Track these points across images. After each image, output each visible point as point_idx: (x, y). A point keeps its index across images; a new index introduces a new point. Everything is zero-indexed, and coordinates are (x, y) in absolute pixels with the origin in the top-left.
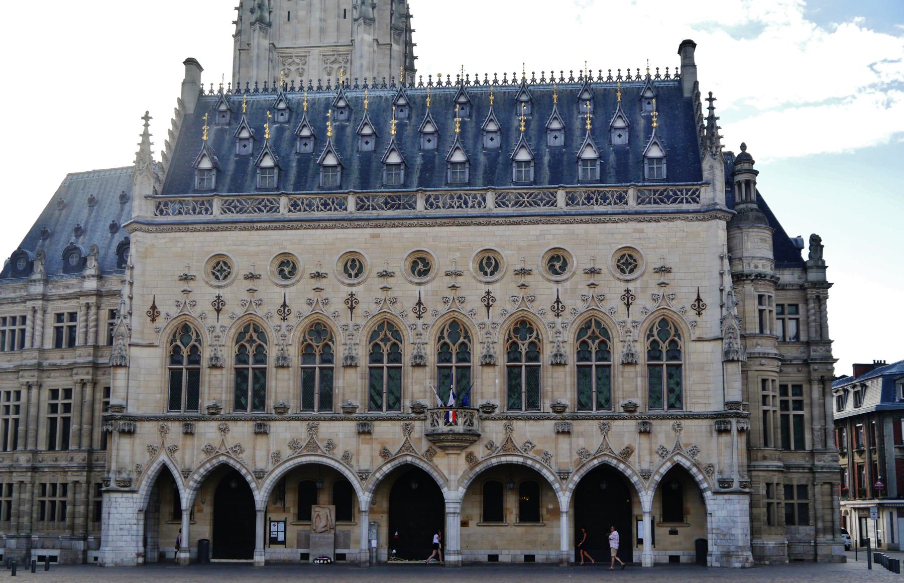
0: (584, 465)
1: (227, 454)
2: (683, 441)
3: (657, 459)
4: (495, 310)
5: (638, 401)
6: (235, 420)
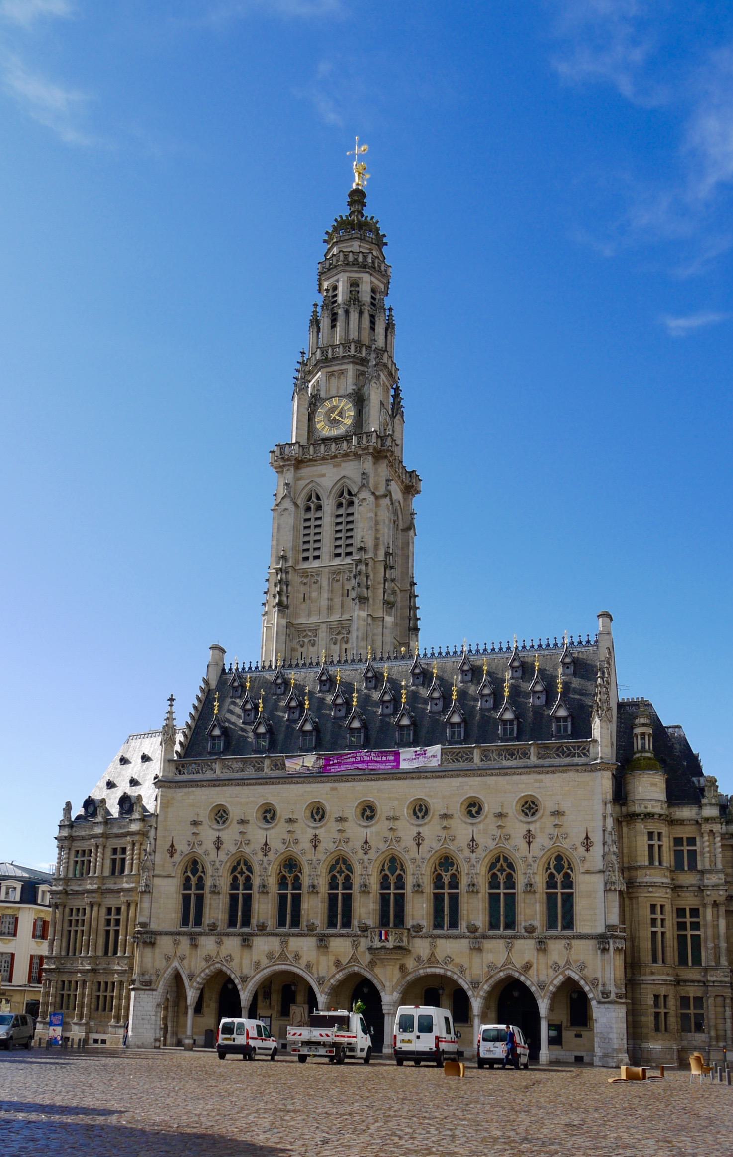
0: (492, 976)
1: (221, 962)
2: (573, 957)
3: (551, 972)
6: (228, 935)
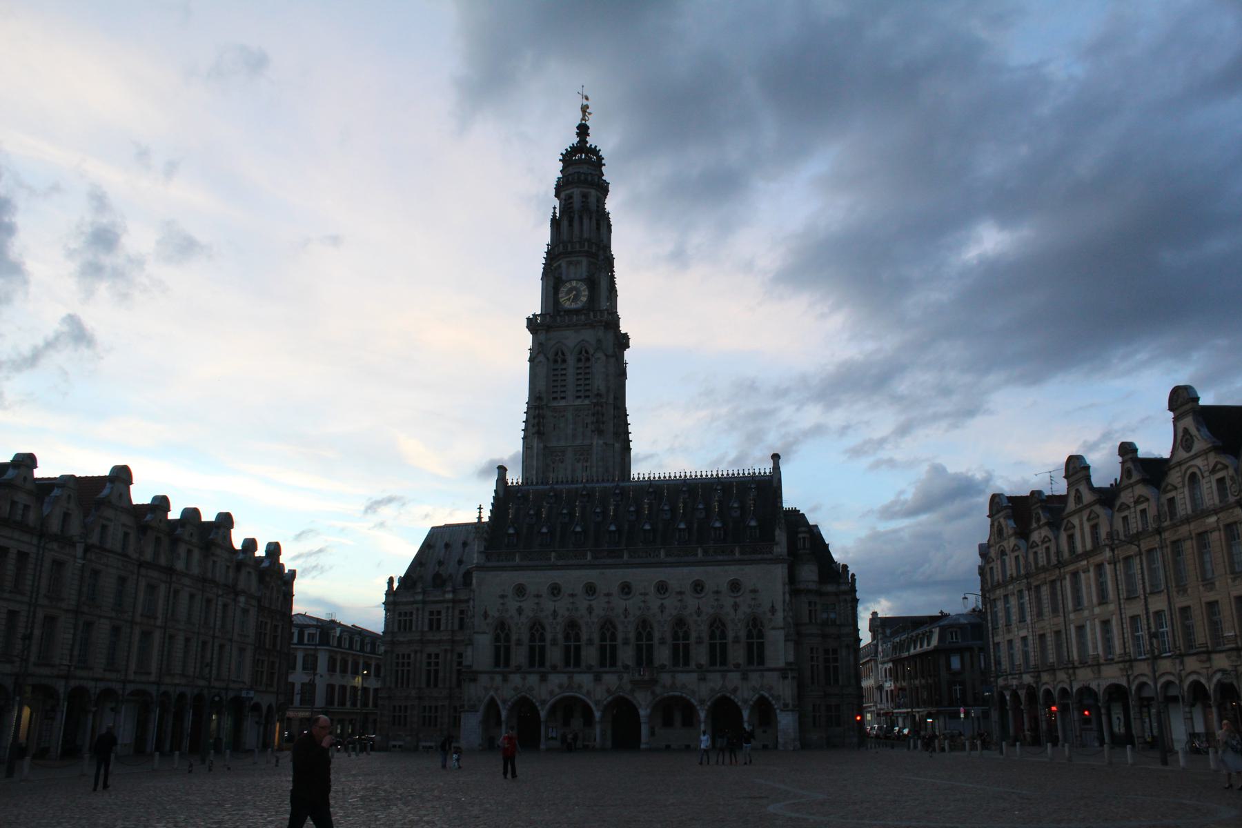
6: (529, 673)
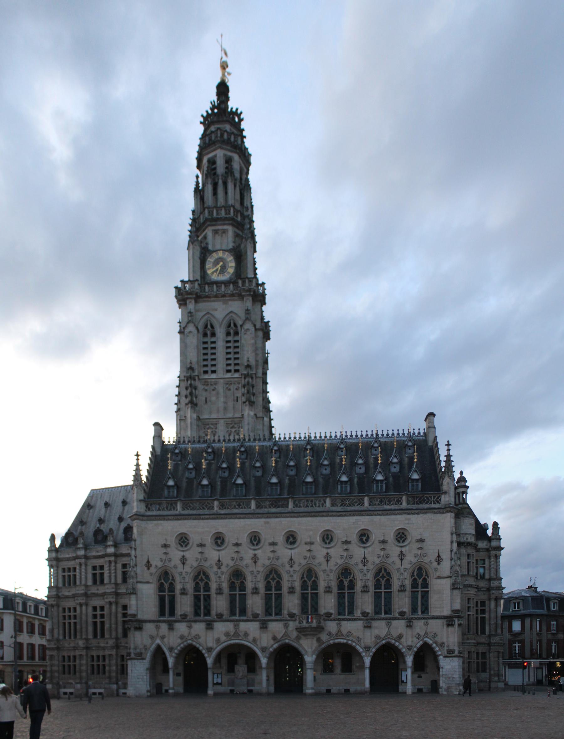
2: (429, 630)
3: (415, 640)
4: (332, 563)
5: (405, 610)
6: (195, 621)
